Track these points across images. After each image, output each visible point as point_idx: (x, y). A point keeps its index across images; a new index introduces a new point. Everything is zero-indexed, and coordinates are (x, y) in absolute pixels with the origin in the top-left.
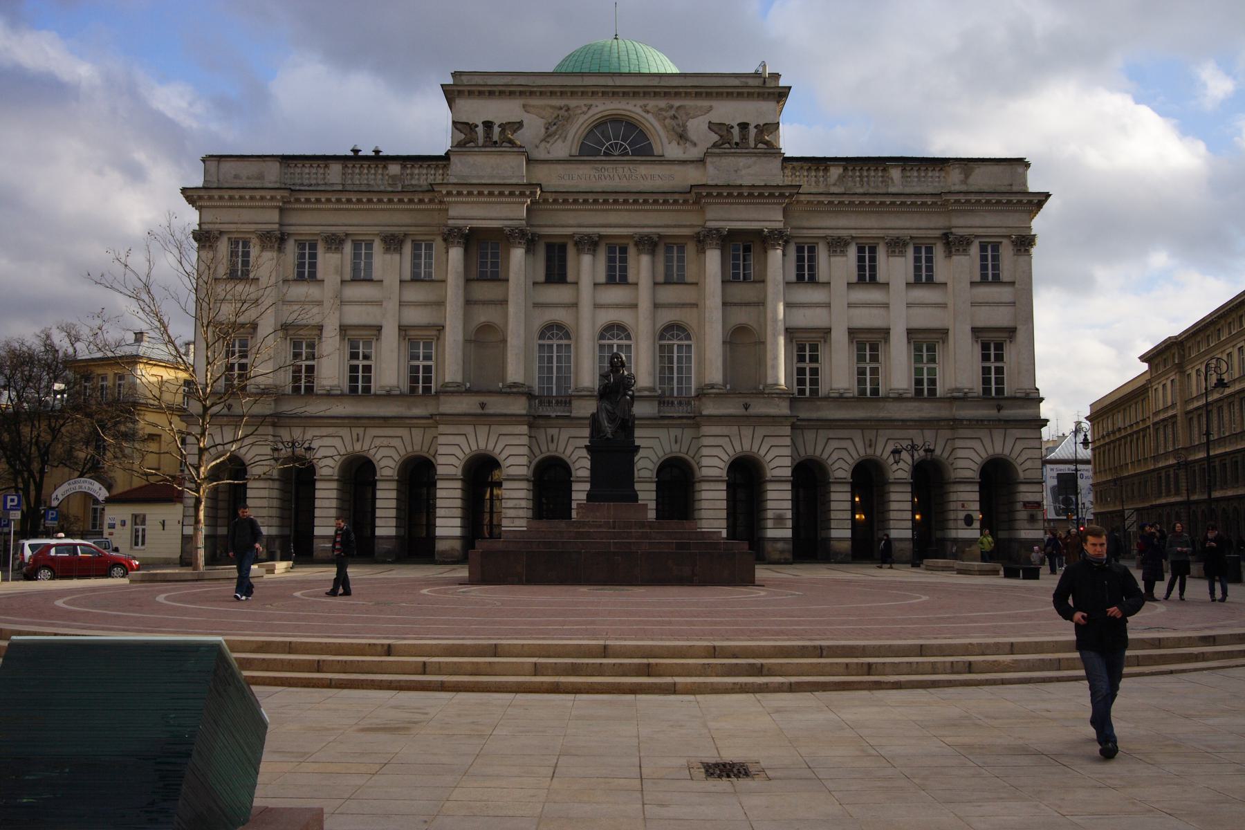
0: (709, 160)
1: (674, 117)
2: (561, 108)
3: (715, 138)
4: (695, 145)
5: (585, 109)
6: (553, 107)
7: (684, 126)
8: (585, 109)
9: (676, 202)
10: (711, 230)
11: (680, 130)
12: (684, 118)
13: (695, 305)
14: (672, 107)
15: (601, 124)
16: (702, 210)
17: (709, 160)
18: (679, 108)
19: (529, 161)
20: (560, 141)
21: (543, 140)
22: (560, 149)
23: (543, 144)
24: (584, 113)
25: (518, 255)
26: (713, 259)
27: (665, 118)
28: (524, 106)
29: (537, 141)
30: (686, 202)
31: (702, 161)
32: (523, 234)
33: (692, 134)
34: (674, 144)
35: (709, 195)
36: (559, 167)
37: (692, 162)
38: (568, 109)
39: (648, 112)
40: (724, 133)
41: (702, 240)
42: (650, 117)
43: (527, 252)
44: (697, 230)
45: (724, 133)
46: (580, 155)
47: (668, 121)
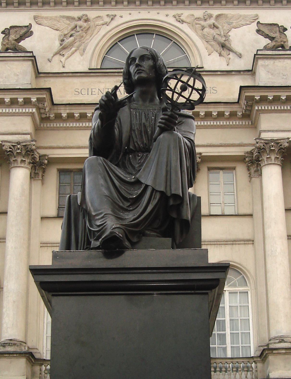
0: (260, 62)
1: (214, 26)
2: (80, 19)
3: (265, 42)
4: (240, 56)
5: (108, 20)
6: (68, 18)
7: (226, 36)
8: (108, 20)
9: (221, 115)
10: (267, 142)
11: (222, 40)
12: (226, 27)
13: (251, 241)
14: (210, 16)
15: (127, 36)
16: (254, 125)
17: (260, 62)
18: (218, 16)
19: (38, 74)
20: (77, 54)
21: (58, 53)
22: (78, 62)
23: (57, 57)
24: (107, 24)
25: (20, 175)
26: (272, 175)
27: (203, 28)
28: (35, 18)
29: (50, 55)
30: (233, 115)
31: (251, 72)
32: (28, 151)
33: (235, 45)
34: (215, 55)
35: (264, 100)
36: (77, 82)
37: (239, 72)
38: (87, 21)
39: (182, 22)
40: (277, 35)
41: (253, 162)
42: (185, 27)
43: (33, 176)
44: (249, 149)
45: (277, 35)
46: (101, 69)
47: (207, 30)
